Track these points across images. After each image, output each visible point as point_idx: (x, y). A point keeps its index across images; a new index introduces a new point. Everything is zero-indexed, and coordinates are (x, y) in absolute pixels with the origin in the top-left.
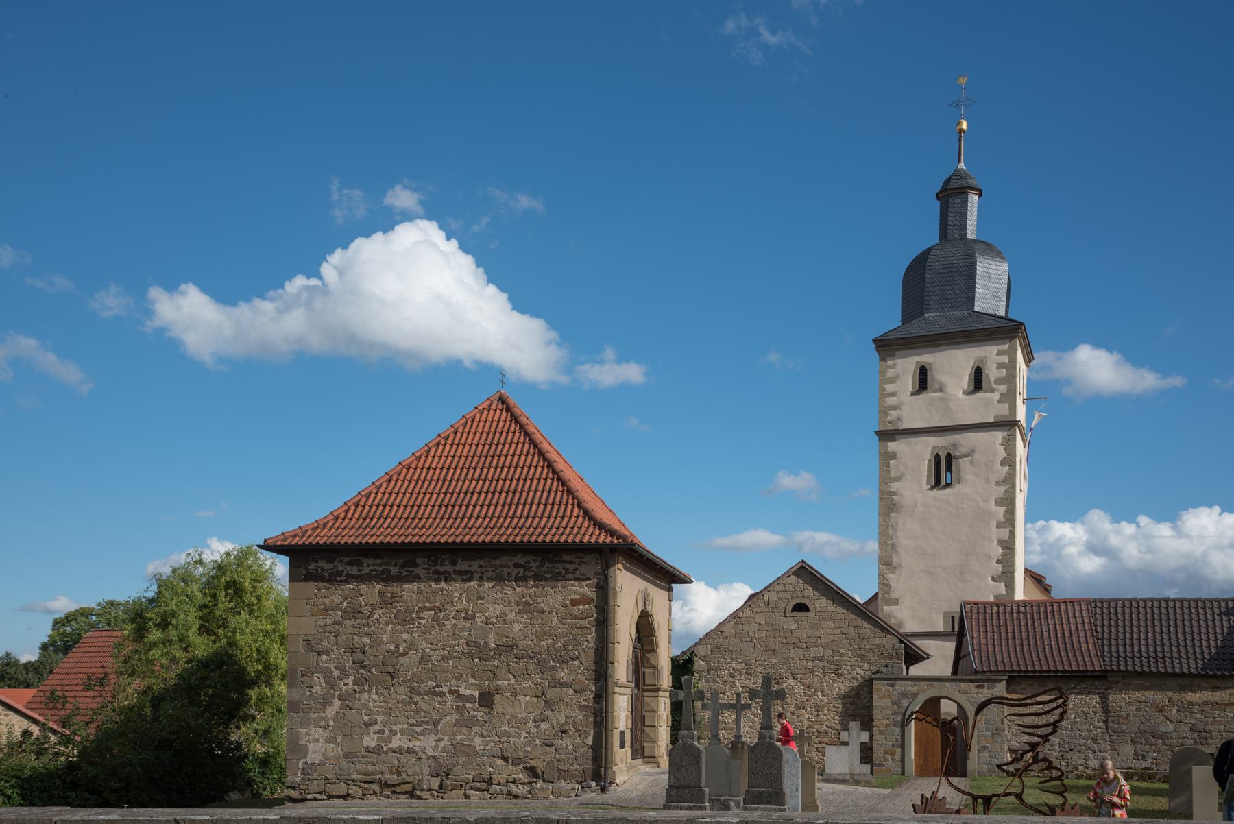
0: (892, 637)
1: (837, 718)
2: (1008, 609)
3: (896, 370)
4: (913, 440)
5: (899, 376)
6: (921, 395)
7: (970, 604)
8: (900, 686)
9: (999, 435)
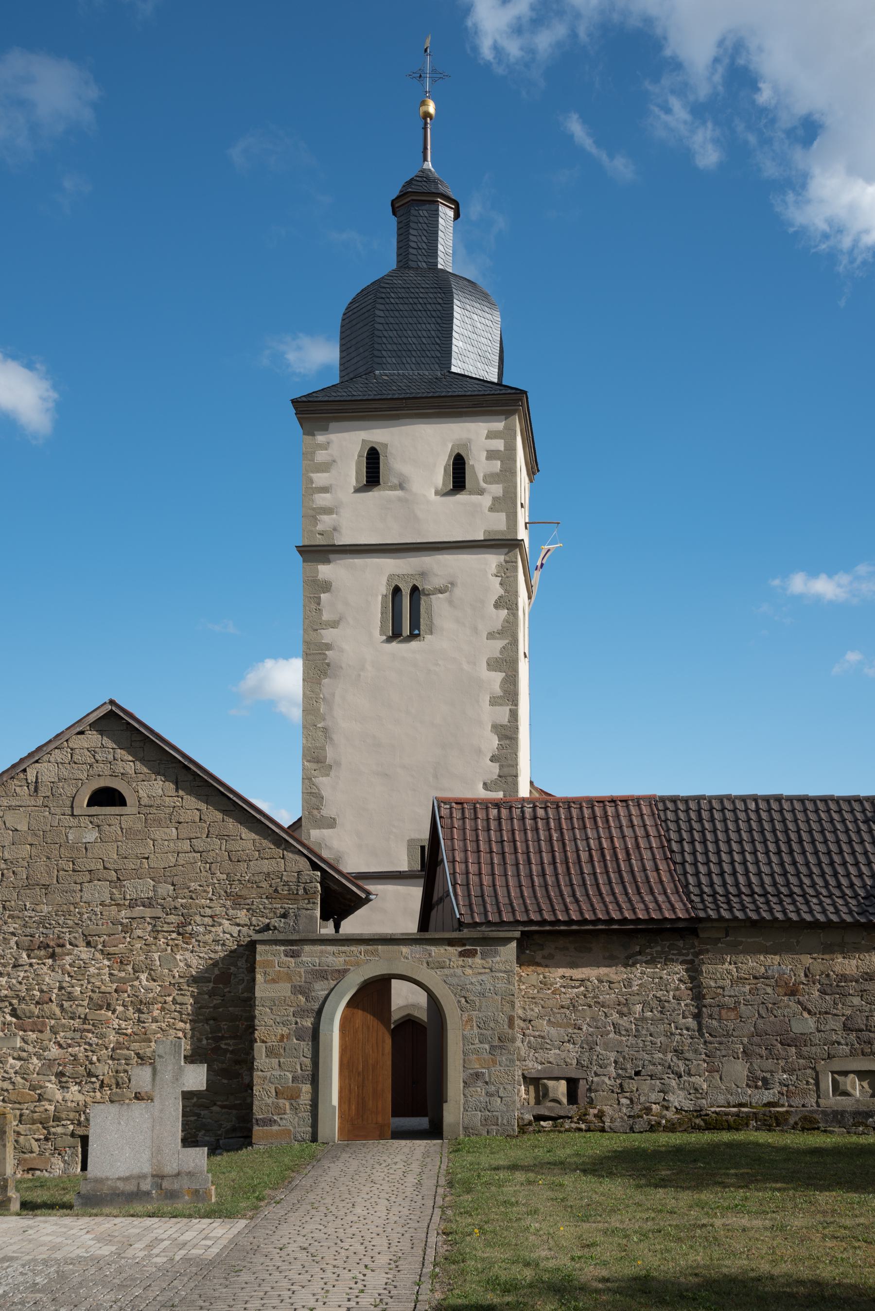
0: (297, 857)
1: (181, 1025)
2: (516, 813)
3: (329, 451)
4: (358, 562)
5: (334, 461)
6: (370, 493)
7: (450, 803)
8: (311, 955)
9: (492, 560)
